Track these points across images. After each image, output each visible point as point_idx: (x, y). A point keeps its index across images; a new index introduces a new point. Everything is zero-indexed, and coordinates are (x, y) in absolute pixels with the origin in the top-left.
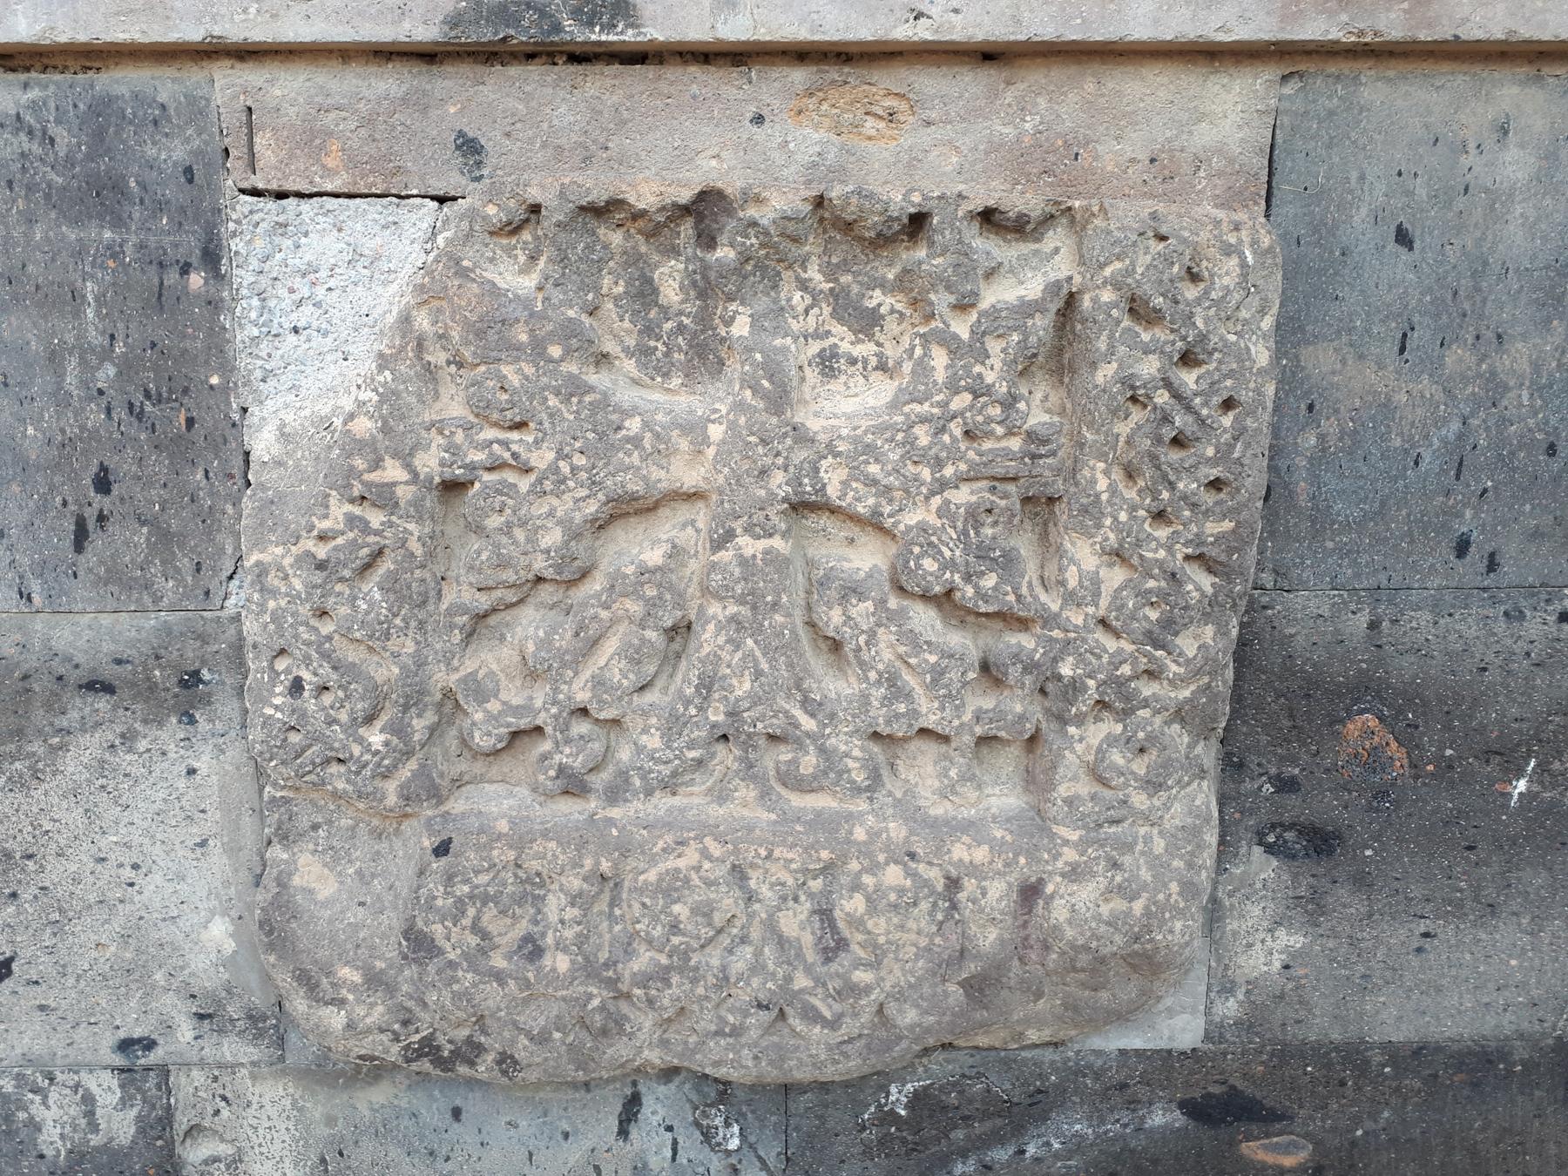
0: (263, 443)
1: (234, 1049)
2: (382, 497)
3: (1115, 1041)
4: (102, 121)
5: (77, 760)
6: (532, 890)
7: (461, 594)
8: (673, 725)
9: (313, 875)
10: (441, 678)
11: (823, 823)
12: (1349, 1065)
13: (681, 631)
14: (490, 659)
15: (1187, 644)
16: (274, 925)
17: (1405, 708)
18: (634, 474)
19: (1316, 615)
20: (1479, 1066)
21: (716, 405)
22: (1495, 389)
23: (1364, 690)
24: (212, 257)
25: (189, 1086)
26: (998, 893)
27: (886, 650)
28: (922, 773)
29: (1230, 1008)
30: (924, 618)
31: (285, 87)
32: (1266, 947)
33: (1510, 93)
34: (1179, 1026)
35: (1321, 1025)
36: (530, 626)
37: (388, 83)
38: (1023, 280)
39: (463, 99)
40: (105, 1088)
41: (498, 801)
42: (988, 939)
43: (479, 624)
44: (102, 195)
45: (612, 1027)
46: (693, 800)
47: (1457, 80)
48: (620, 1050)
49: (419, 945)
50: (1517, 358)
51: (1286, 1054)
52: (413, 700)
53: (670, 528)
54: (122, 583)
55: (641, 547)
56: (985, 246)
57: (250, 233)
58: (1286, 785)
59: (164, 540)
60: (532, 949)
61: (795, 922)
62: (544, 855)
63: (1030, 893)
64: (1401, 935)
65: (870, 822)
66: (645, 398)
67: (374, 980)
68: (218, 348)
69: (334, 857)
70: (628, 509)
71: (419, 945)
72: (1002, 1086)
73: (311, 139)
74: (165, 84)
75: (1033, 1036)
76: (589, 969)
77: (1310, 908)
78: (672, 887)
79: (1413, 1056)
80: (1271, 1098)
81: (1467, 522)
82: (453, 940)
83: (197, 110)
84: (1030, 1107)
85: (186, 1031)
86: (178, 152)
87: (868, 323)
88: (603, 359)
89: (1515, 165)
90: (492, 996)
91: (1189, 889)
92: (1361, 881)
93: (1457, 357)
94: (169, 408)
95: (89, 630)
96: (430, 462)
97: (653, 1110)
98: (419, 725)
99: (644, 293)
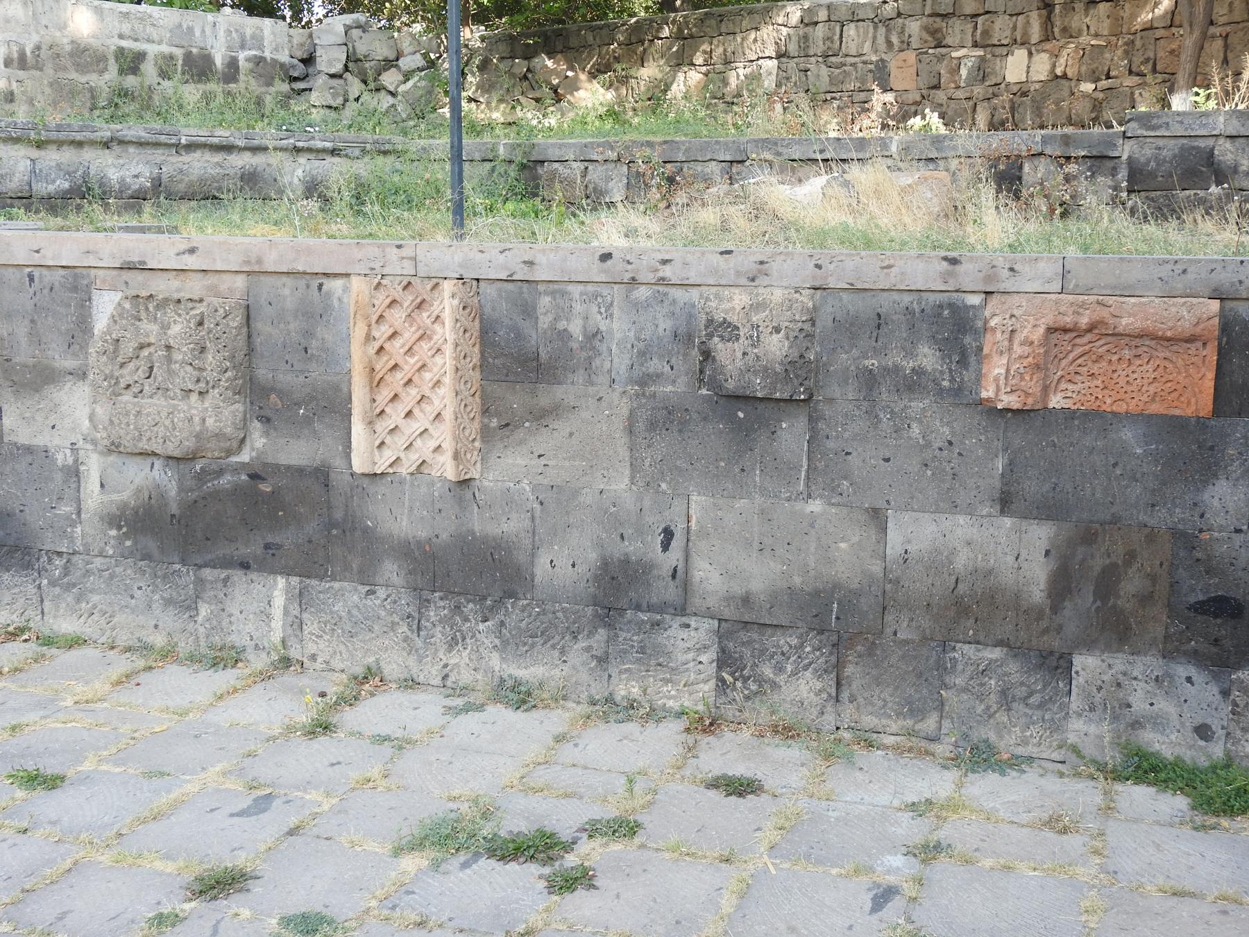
0: (96, 332)
1: (89, 447)
2: (106, 341)
3: (234, 459)
4: (76, 276)
5: (69, 385)
6: (127, 414)
7: (120, 359)
8: (150, 385)
9: (99, 410)
10: (116, 374)
11: (174, 406)
12: (277, 467)
13: (151, 368)
14: (125, 371)
15: (227, 375)
16: (91, 418)
17: (281, 394)
18: (143, 340)
19: (263, 373)
20: (300, 471)
21: (154, 328)
22: (289, 333)
23: (273, 389)
24: (90, 299)
25: (81, 452)
26: (197, 419)
27: (182, 373)
28: (194, 397)
29: (254, 454)
30: (189, 368)
31: (101, 273)
32: (258, 440)
33: (284, 279)
34: (245, 457)
35: (270, 460)
36: (131, 366)
37: (115, 272)
38: (200, 309)
39: (127, 275)
40: (68, 452)
41: (127, 397)
42: (198, 428)
43: (122, 365)
44: (75, 289)
45: (140, 439)
46: (155, 401)
47: (276, 276)
48: (141, 445)
49: (111, 422)
50: (292, 326)
51: (265, 465)
52: (112, 377)
53: (152, 349)
54: (75, 355)
55: (145, 352)
56: (190, 305)
57: (95, 295)
58: (261, 408)
59: (81, 348)
60: (128, 424)
61: (167, 422)
62: (129, 407)
63: (204, 420)
64: (283, 441)
65: (183, 406)
66: (145, 326)
67: (105, 428)
68: (90, 315)
69: (102, 406)
70: (141, 347)
71: (111, 422)
72: (214, 467)
73: (104, 281)
74: (84, 272)
75: (216, 454)
76: (136, 429)
77: (266, 434)
78: (148, 415)
79: (288, 467)
80: (263, 475)
81: (287, 358)
82: (116, 422)
83: (89, 275)
84: (220, 472)
85: (81, 442)
86: (85, 282)
87: (180, 315)
88: (140, 320)
89: (287, 292)
90: (122, 432)
91: (233, 423)
92: (275, 429)
93: (282, 325)
94: (84, 324)
95: (70, 364)
96: (114, 336)
97: (156, 466)
98: (113, 382)
99: (147, 309)
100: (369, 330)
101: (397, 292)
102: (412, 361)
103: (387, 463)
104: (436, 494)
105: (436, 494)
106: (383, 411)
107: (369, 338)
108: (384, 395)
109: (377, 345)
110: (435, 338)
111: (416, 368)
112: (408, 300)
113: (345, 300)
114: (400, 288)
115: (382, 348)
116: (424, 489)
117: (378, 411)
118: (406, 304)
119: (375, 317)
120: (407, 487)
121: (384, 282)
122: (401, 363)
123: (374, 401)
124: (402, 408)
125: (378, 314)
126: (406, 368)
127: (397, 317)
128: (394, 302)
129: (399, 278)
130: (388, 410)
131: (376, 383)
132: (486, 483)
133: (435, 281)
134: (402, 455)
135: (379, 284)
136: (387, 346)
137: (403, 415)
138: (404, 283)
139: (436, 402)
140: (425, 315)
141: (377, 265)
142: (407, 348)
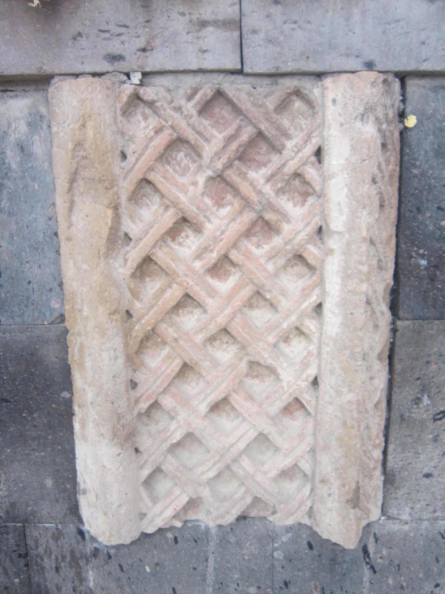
100: (117, 218)
101: (185, 117)
102: (224, 286)
103: (169, 512)
104: (278, 555)
105: (278, 555)
106: (155, 405)
107: (117, 238)
108: (158, 363)
109: (135, 254)
110: (286, 227)
111: (237, 302)
112: (215, 140)
113: (38, 148)
114: (190, 107)
115: (148, 260)
116: (250, 548)
117: (144, 406)
118: (208, 151)
119: (126, 186)
120: (212, 546)
121: (148, 93)
122: (199, 292)
123: (134, 385)
124: (199, 393)
125: (136, 175)
126: (211, 303)
127: (187, 185)
128: (178, 142)
129: (190, 81)
130: (167, 402)
131: (140, 345)
132: (395, 527)
133: (290, 83)
134: (206, 493)
135: (136, 98)
136: (161, 256)
137: (203, 408)
138: (207, 91)
139: (287, 375)
140: (258, 175)
141: (128, 46)
142: (214, 256)
